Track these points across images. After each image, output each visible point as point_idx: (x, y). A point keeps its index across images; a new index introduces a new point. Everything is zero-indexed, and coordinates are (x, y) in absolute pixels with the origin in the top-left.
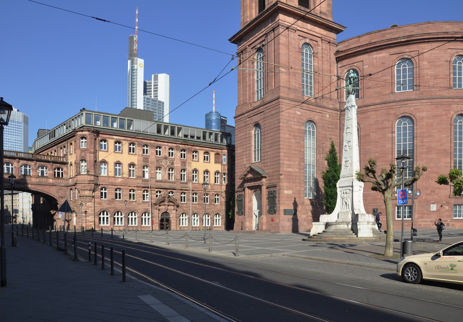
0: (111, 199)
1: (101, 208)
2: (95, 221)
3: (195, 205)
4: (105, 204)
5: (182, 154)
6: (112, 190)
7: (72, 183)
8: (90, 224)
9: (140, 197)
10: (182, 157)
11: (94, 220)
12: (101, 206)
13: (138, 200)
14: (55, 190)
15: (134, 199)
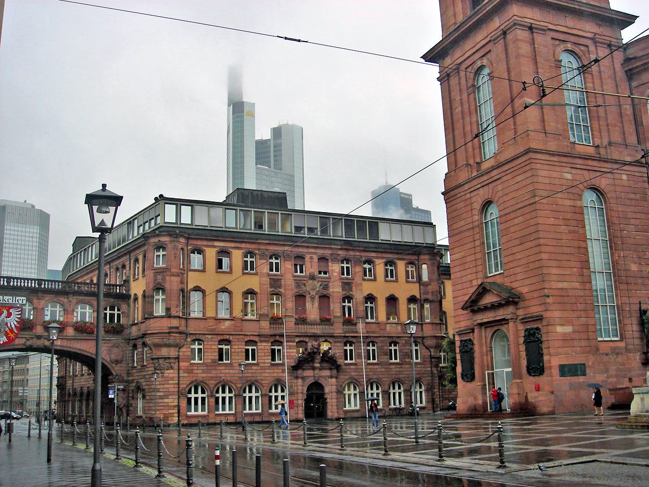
1: (191, 379)
2: (179, 406)
3: (371, 367)
5: (343, 268)
6: (214, 343)
7: (136, 334)
8: (170, 411)
9: (266, 355)
10: (343, 274)
11: (177, 404)
15: (253, 359)
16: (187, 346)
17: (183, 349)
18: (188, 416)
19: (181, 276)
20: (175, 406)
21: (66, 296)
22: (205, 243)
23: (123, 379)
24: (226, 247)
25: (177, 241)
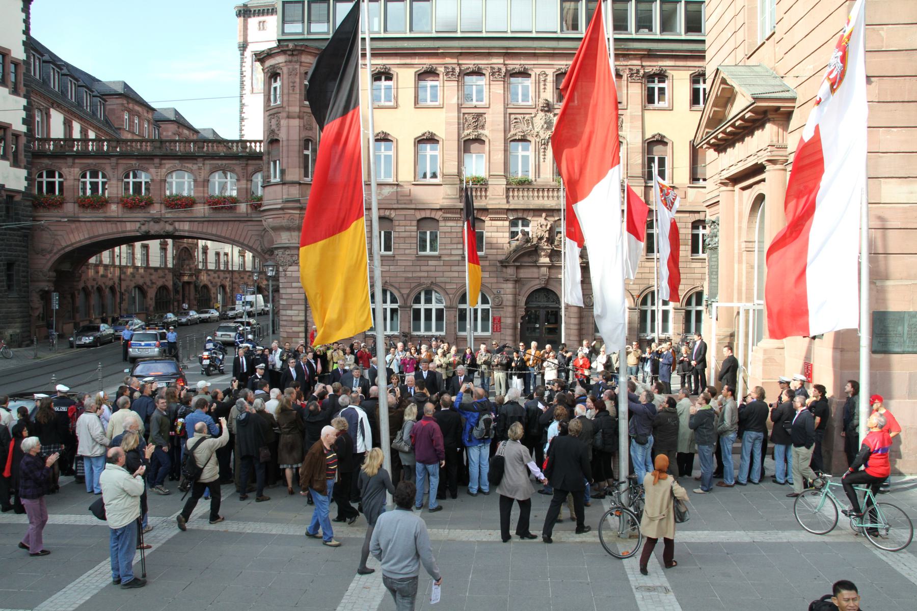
8: (295, 329)
9: (455, 241)
11: (303, 318)
13: (448, 252)
14: (254, 233)
15: (433, 248)
20: (300, 322)
21: (195, 162)
25: (296, 62)
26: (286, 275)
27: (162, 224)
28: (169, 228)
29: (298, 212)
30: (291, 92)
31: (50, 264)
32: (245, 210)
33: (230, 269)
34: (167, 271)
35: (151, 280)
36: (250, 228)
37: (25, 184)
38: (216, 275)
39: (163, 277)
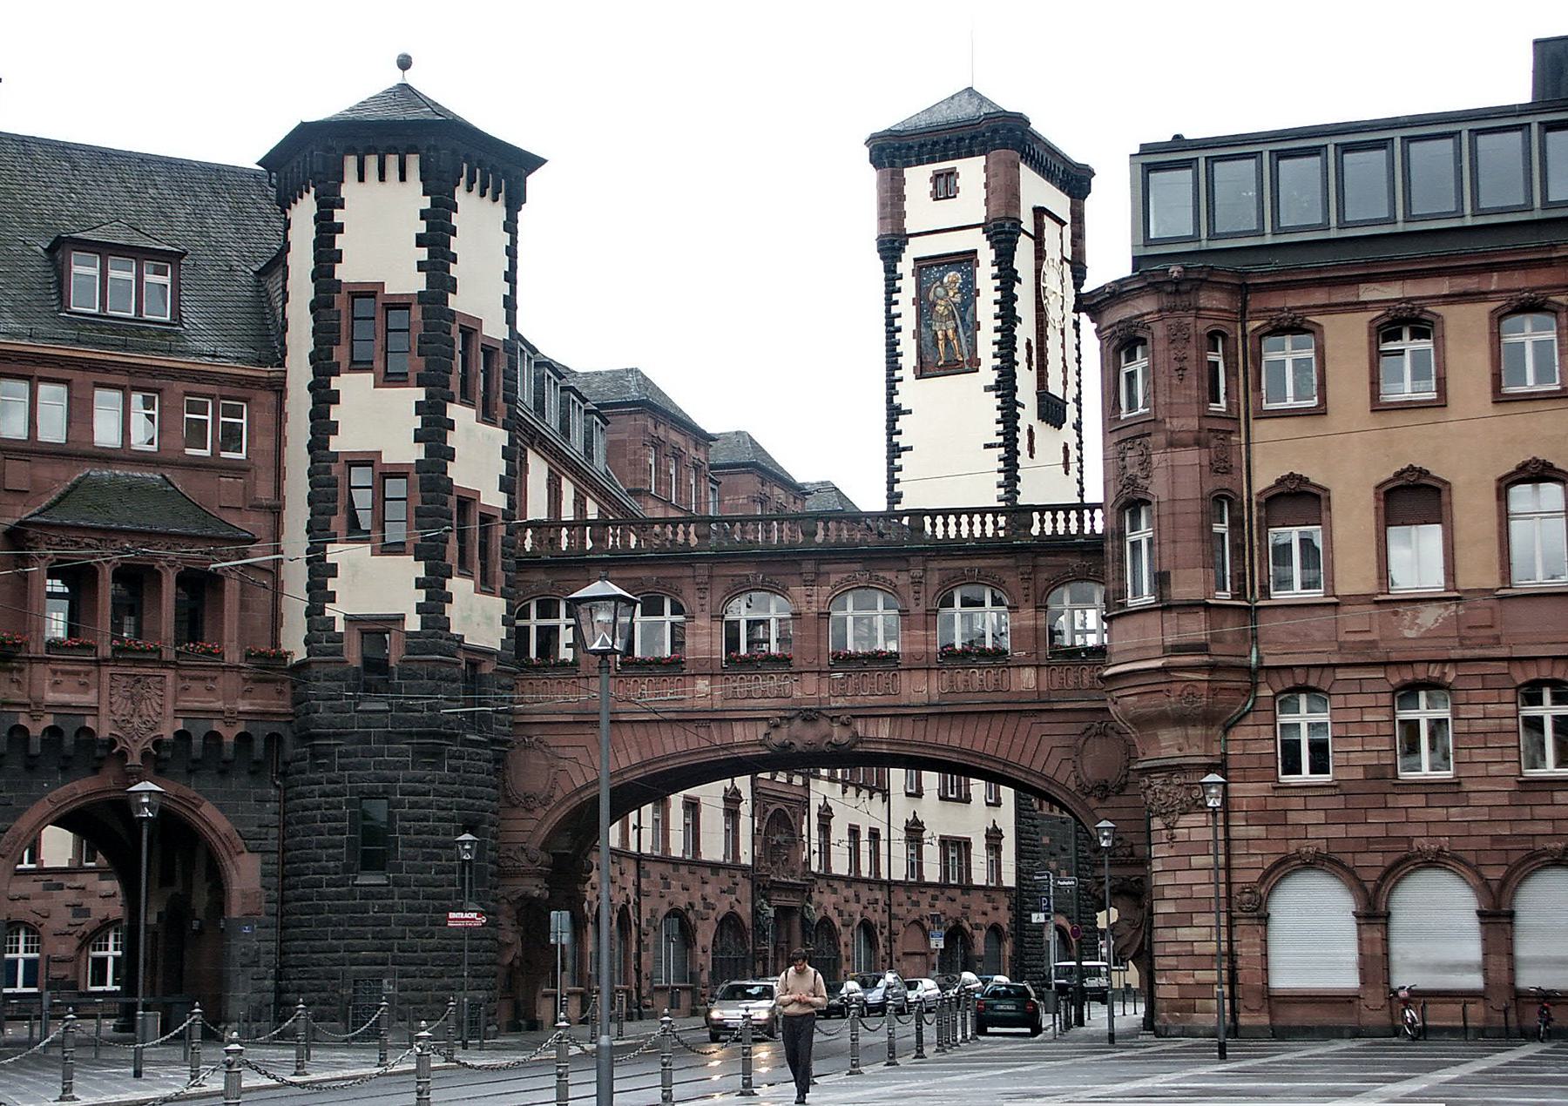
0: (1359, 774)
2: (1231, 955)
4: (1310, 817)
8: (1202, 976)
12: (1277, 832)
14: (1056, 741)
16: (1264, 717)
17: (1240, 733)
18: (1270, 997)
19: (1214, 442)
21: (904, 565)
22: (1319, 297)
23: (1132, 854)
24: (1409, 300)
25: (1186, 309)
26: (1173, 837)
27: (824, 725)
28: (839, 734)
29: (1206, 677)
30: (1175, 382)
31: (544, 831)
32: (1032, 684)
33: (884, 876)
34: (739, 875)
35: (704, 899)
36: (1047, 729)
37: (502, 632)
38: (850, 893)
39: (731, 891)
